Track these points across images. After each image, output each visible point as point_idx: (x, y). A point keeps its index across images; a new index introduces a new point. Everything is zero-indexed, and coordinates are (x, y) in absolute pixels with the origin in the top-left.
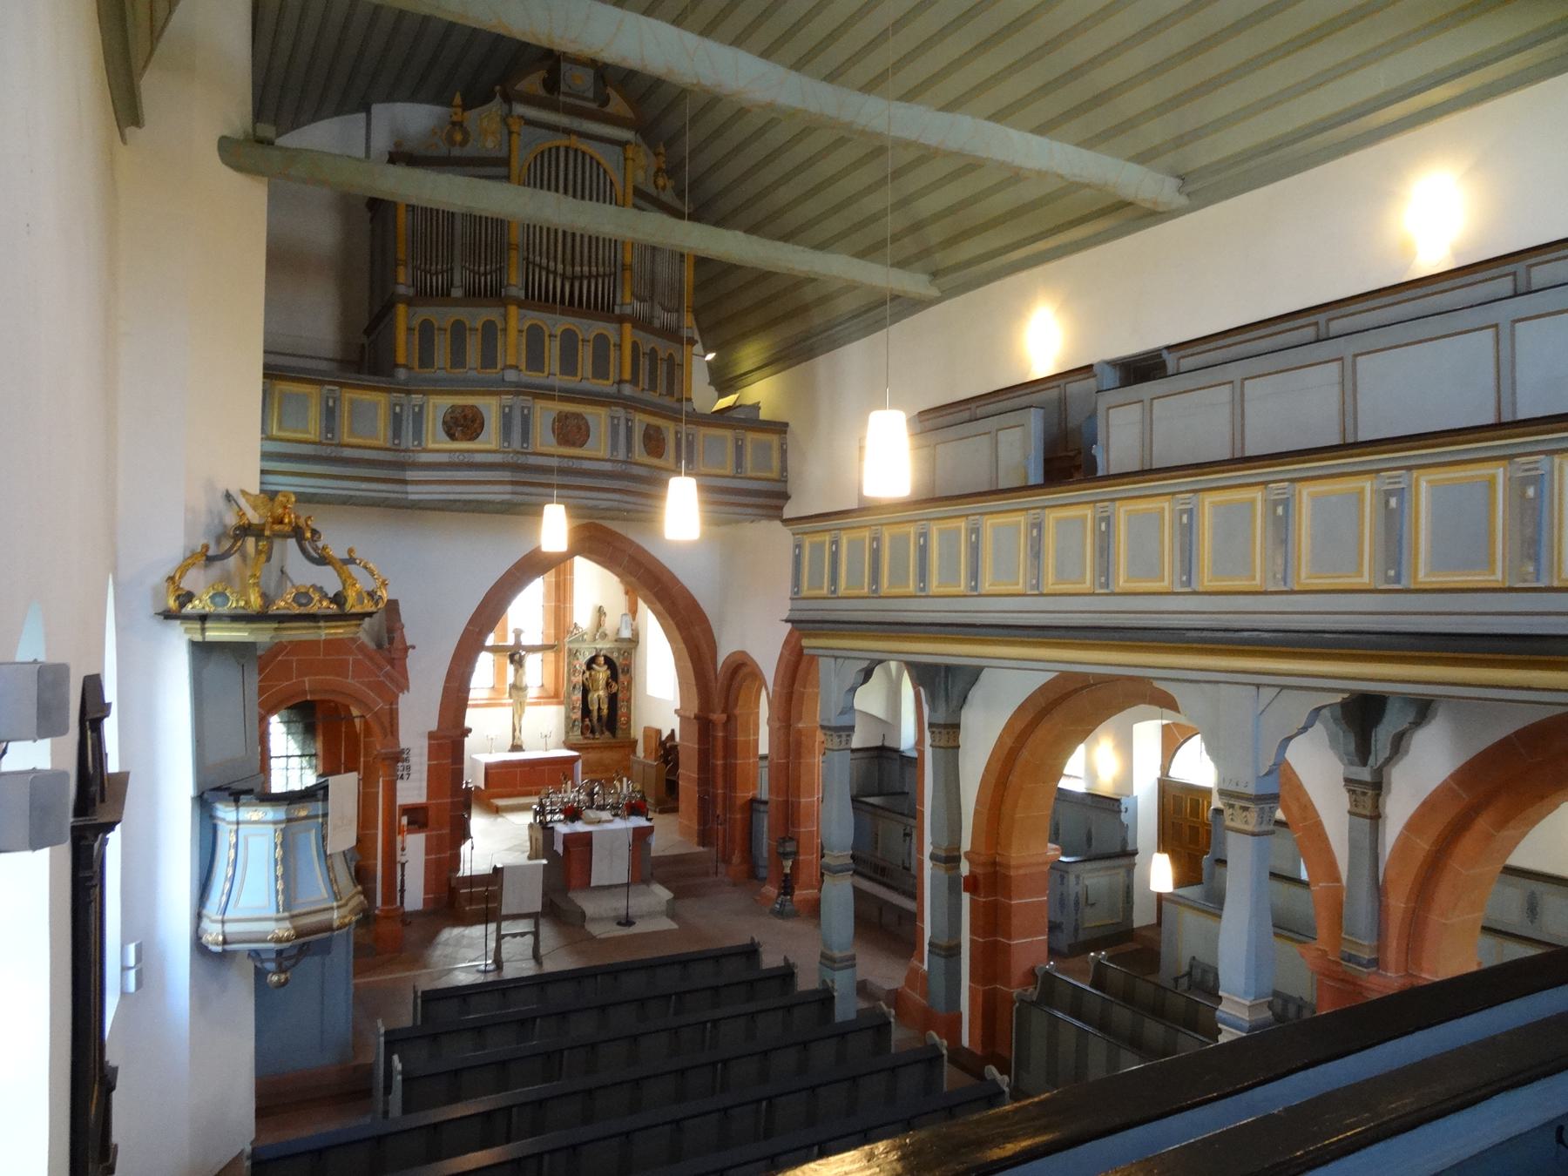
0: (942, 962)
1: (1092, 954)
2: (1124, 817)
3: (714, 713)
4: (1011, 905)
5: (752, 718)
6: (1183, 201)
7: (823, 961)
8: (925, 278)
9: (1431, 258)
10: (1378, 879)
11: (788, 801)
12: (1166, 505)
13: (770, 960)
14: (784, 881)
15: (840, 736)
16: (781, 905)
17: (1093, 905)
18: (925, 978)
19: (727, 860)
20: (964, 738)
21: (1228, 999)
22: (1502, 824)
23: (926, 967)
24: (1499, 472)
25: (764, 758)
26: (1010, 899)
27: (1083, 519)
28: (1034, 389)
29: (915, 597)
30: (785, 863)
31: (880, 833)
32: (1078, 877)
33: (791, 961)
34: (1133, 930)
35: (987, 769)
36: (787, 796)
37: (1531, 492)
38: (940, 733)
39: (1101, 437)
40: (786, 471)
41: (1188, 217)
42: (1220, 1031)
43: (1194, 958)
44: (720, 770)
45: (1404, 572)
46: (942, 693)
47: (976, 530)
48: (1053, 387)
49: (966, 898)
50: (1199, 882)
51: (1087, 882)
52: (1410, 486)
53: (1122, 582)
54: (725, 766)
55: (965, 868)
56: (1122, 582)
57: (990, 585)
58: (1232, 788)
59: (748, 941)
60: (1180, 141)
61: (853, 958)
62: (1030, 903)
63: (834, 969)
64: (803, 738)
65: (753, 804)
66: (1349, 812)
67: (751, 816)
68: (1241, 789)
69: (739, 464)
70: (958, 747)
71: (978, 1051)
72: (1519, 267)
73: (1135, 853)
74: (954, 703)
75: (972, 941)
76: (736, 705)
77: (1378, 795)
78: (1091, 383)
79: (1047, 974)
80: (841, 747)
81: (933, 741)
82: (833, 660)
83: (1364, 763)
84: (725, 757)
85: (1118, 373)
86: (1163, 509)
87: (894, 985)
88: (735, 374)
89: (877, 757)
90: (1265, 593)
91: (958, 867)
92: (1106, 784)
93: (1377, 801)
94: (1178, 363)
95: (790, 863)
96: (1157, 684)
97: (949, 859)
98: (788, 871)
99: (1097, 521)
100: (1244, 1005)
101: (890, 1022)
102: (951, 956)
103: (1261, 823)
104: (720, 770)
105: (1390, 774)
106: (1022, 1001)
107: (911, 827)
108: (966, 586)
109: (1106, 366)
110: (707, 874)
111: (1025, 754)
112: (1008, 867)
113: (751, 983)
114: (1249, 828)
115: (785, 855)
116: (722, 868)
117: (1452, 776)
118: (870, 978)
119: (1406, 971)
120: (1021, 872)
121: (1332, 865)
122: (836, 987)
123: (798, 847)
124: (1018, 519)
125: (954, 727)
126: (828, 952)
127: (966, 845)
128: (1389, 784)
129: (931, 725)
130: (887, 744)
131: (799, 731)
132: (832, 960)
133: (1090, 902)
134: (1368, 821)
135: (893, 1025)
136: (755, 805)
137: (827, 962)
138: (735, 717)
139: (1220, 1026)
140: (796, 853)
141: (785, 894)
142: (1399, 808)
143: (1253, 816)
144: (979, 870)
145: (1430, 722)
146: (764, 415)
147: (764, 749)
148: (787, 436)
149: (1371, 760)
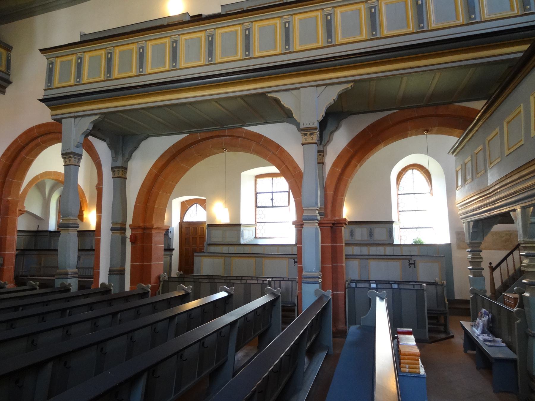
15: (75, 158)
27: (236, 32)
38: (118, 171)
46: (121, 152)
55: (128, 233)
64: (10, 205)
70: (126, 179)
74: (127, 156)
81: (114, 174)
82: (73, 119)
86: (276, 23)
96: (270, 95)
105: (326, 148)
117: (347, 145)
122: (72, 284)
125: (125, 169)
127: (129, 221)
130: (40, 229)
131: (8, 201)
142: (330, 159)
145: (339, 129)
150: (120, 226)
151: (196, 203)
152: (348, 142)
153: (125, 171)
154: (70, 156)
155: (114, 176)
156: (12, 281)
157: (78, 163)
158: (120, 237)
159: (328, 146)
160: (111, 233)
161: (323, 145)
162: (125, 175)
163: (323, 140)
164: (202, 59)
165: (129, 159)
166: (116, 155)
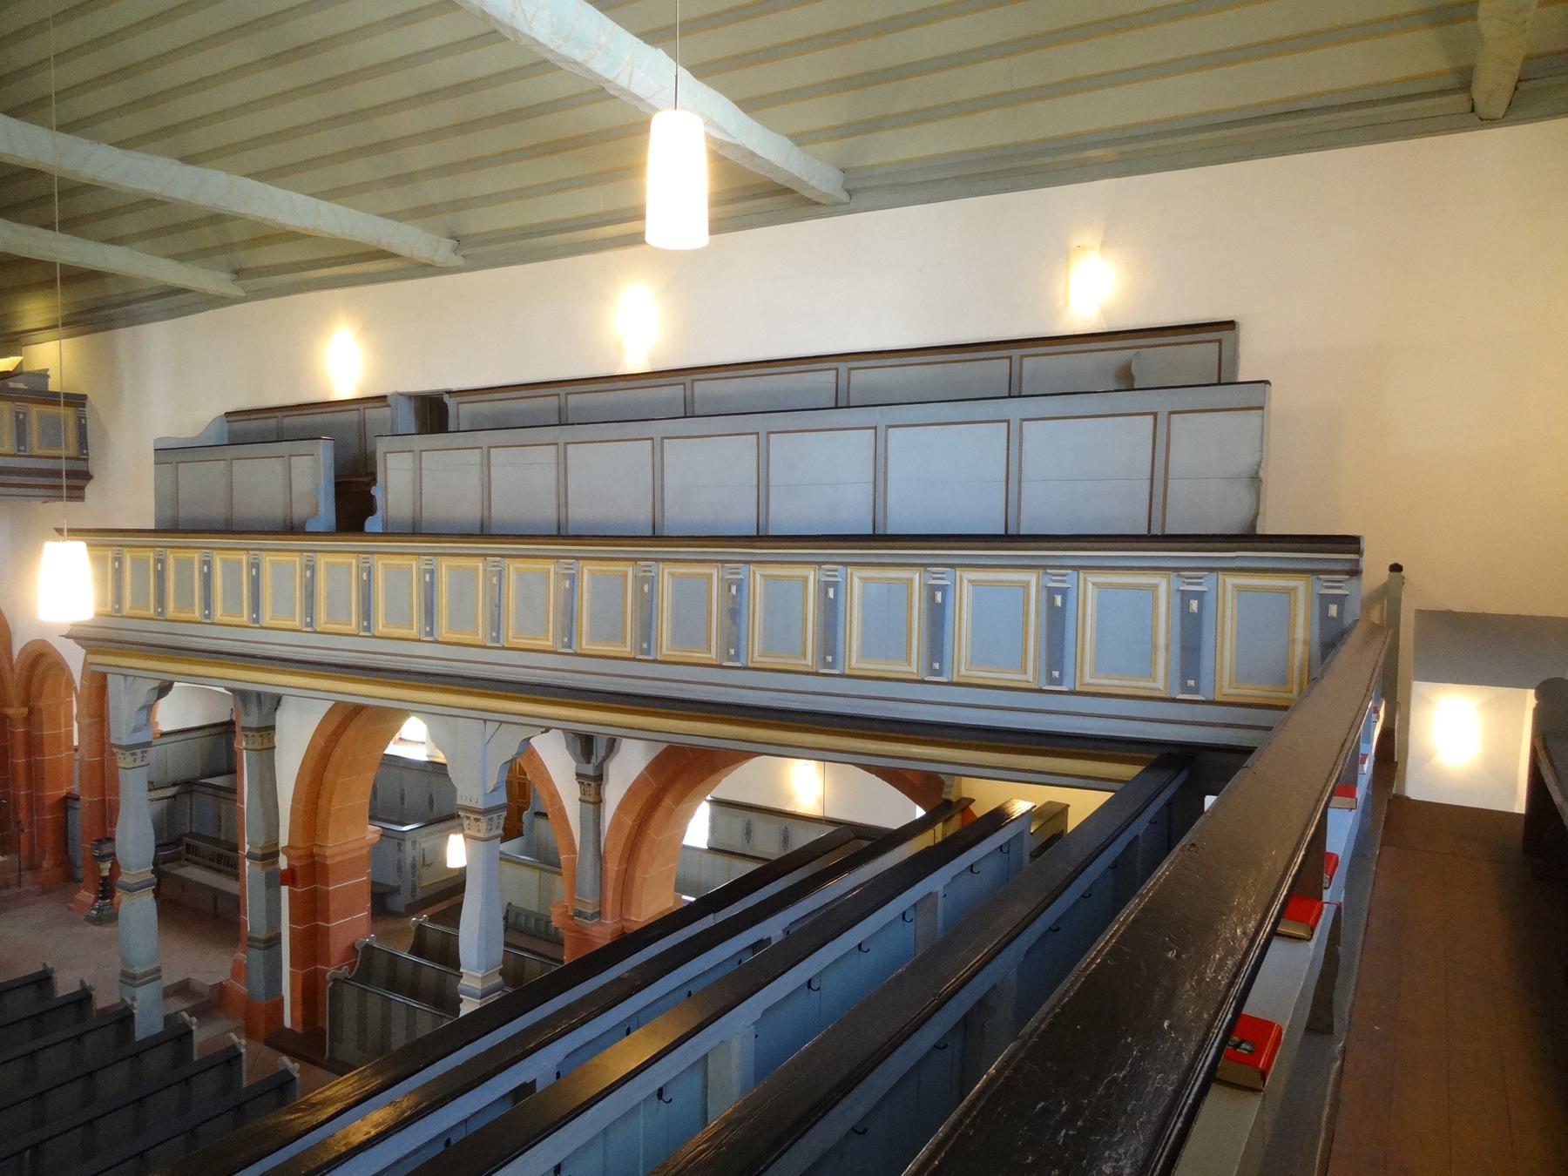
3: (11, 706)
4: (328, 891)
5: (62, 709)
6: (457, 261)
7: (124, 979)
8: (226, 276)
9: (635, 362)
11: (104, 800)
12: (414, 563)
13: (65, 985)
14: (102, 885)
16: (99, 910)
17: (429, 865)
19: (33, 867)
20: (279, 739)
24: (629, 569)
25: (76, 750)
26: (328, 885)
28: (333, 409)
29: (200, 623)
32: (414, 843)
33: (88, 984)
36: (104, 795)
37: (646, 588)
38: (253, 736)
40: (87, 448)
42: (461, 1000)
43: (510, 904)
44: (21, 771)
45: (574, 644)
47: (256, 565)
48: (354, 410)
50: (520, 834)
51: (423, 846)
52: (578, 572)
53: (380, 627)
54: (29, 766)
55: (283, 863)
60: (457, 205)
61: (158, 970)
65: (68, 801)
66: (580, 800)
67: (67, 814)
69: (21, 438)
70: (274, 747)
71: (299, 1030)
72: (687, 379)
76: (39, 697)
77: (600, 785)
78: (386, 412)
79: (368, 947)
80: (137, 764)
82: (122, 678)
83: (589, 762)
84: (29, 754)
85: (413, 405)
87: (221, 979)
88: (21, 329)
89: (226, 732)
90: (485, 647)
91: (277, 862)
94: (458, 407)
95: (109, 865)
97: (269, 856)
98: (106, 873)
100: (477, 977)
103: (491, 829)
104: (21, 771)
105: (608, 764)
106: (335, 980)
108: (249, 618)
109: (402, 400)
110: (7, 886)
111: (338, 750)
112: (325, 857)
114: (480, 835)
115: (103, 858)
116: (27, 876)
117: (646, 769)
118: (193, 976)
119: (621, 916)
120: (339, 859)
122: (135, 1005)
125: (273, 728)
127: (284, 840)
128: (608, 775)
132: (134, 978)
133: (427, 863)
134: (591, 806)
136: (71, 803)
137: (128, 981)
138: (41, 710)
139: (461, 996)
141: (102, 899)
142: (614, 793)
143: (483, 825)
144: (297, 864)
146: (53, 385)
147: (76, 743)
148: (86, 410)
149: (593, 760)
157: (142, 760)
159: (611, 761)
162: (271, 739)
163: (595, 753)
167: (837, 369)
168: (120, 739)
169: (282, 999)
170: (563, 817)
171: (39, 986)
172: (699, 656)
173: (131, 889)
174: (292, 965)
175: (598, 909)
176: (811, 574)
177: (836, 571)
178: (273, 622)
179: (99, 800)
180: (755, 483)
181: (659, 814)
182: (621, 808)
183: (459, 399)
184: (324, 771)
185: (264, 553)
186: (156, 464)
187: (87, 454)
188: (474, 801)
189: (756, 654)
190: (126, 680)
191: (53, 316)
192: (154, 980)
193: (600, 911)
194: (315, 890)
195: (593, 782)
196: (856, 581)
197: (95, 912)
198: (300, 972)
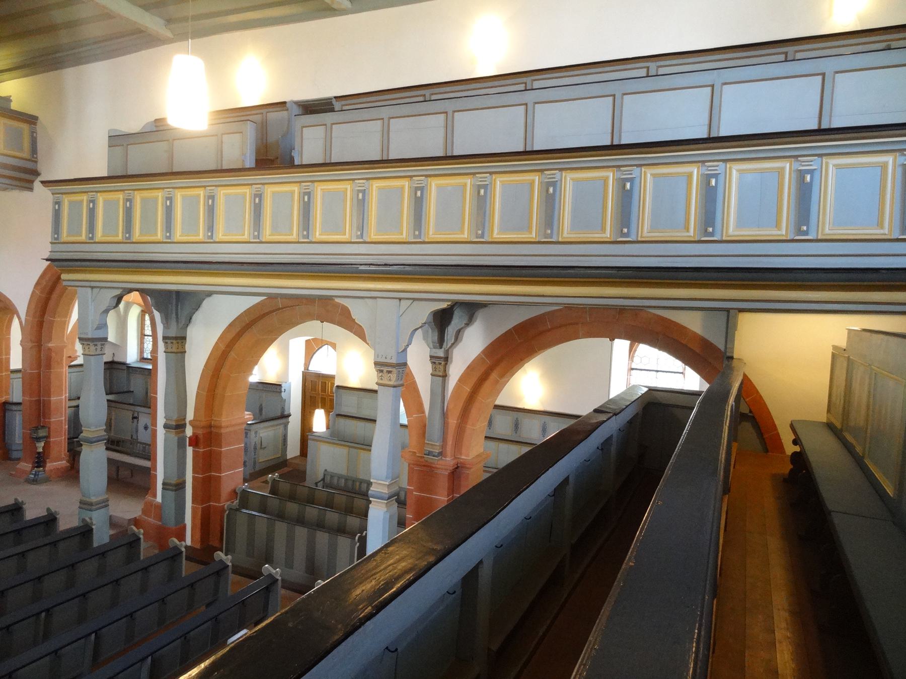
0: (171, 494)
1: (270, 476)
2: (283, 394)
4: (221, 452)
5: (4, 343)
7: (82, 506)
10: (444, 407)
11: (39, 401)
15: (96, 345)
16: (35, 475)
18: (159, 507)
21: (374, 482)
22: (502, 375)
23: (159, 499)
24: (536, 178)
26: (221, 448)
27: (293, 192)
30: (38, 445)
31: (113, 418)
32: (256, 433)
34: (286, 460)
35: (206, 366)
36: (39, 396)
38: (172, 343)
39: (297, 147)
40: (36, 154)
41: (350, 16)
42: (370, 502)
43: (326, 470)
46: (174, 315)
49: (190, 451)
51: (261, 435)
52: (491, 183)
55: (189, 431)
56: (318, 235)
57: (222, 236)
58: (383, 360)
59: (12, 502)
62: (231, 449)
63: (91, 510)
68: (388, 361)
70: (185, 352)
71: (198, 546)
73: (289, 415)
74: (183, 321)
75: (194, 478)
77: (446, 364)
81: (166, 347)
82: (89, 290)
86: (346, 189)
91: (184, 431)
92: (271, 378)
93: (445, 368)
95: (42, 444)
96: (337, 300)
97: (179, 427)
98: (41, 450)
99: (302, 195)
101: (139, 539)
102: (180, 489)
107: (138, 413)
111: (232, 355)
113: (18, 532)
115: (38, 439)
117: (484, 352)
121: (421, 405)
122: (94, 523)
123: (49, 433)
124: (245, 190)
125: (182, 339)
126: (84, 499)
127: (190, 416)
128: (452, 358)
129: (165, 338)
130: (116, 359)
131: (50, 349)
132: (91, 504)
133: (263, 447)
134: (441, 378)
135: (142, 540)
136: (7, 407)
139: (371, 499)
140: (48, 437)
141: (37, 467)
142: (456, 370)
143: (393, 376)
145: (474, 323)
146: (14, 106)
149: (445, 344)
150: (175, 424)
151: (327, 344)
152: (486, 346)
153: (182, 342)
154: (89, 343)
155: (167, 351)
156: (63, 456)
158: (176, 438)
159: (455, 347)
160: (165, 432)
161: (445, 349)
162: (183, 346)
164: (246, 233)
165: (187, 326)
166: (167, 323)
167: (648, 68)
168: (87, 334)
169: (184, 527)
170: (414, 388)
171: (13, 514)
172: (597, 236)
173: (90, 442)
174: (194, 501)
175: (441, 450)
176: (695, 170)
177: (717, 166)
178: (226, 237)
179: (36, 400)
180: (610, 131)
181: (487, 385)
182: (462, 380)
183: (343, 102)
184: (221, 368)
185: (219, 188)
186: (109, 147)
187: (36, 158)
188: (389, 357)
189: (645, 230)
190: (92, 290)
191: (15, 61)
192: (102, 507)
193: (442, 452)
194: (211, 450)
195: (440, 363)
196: (734, 172)
197: (33, 476)
198: (200, 507)
